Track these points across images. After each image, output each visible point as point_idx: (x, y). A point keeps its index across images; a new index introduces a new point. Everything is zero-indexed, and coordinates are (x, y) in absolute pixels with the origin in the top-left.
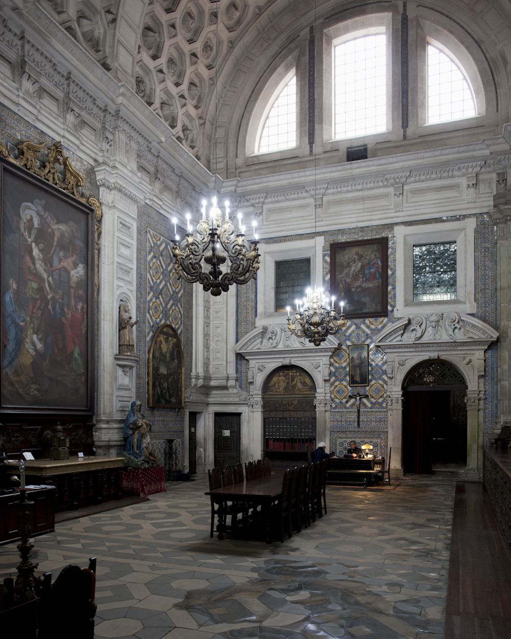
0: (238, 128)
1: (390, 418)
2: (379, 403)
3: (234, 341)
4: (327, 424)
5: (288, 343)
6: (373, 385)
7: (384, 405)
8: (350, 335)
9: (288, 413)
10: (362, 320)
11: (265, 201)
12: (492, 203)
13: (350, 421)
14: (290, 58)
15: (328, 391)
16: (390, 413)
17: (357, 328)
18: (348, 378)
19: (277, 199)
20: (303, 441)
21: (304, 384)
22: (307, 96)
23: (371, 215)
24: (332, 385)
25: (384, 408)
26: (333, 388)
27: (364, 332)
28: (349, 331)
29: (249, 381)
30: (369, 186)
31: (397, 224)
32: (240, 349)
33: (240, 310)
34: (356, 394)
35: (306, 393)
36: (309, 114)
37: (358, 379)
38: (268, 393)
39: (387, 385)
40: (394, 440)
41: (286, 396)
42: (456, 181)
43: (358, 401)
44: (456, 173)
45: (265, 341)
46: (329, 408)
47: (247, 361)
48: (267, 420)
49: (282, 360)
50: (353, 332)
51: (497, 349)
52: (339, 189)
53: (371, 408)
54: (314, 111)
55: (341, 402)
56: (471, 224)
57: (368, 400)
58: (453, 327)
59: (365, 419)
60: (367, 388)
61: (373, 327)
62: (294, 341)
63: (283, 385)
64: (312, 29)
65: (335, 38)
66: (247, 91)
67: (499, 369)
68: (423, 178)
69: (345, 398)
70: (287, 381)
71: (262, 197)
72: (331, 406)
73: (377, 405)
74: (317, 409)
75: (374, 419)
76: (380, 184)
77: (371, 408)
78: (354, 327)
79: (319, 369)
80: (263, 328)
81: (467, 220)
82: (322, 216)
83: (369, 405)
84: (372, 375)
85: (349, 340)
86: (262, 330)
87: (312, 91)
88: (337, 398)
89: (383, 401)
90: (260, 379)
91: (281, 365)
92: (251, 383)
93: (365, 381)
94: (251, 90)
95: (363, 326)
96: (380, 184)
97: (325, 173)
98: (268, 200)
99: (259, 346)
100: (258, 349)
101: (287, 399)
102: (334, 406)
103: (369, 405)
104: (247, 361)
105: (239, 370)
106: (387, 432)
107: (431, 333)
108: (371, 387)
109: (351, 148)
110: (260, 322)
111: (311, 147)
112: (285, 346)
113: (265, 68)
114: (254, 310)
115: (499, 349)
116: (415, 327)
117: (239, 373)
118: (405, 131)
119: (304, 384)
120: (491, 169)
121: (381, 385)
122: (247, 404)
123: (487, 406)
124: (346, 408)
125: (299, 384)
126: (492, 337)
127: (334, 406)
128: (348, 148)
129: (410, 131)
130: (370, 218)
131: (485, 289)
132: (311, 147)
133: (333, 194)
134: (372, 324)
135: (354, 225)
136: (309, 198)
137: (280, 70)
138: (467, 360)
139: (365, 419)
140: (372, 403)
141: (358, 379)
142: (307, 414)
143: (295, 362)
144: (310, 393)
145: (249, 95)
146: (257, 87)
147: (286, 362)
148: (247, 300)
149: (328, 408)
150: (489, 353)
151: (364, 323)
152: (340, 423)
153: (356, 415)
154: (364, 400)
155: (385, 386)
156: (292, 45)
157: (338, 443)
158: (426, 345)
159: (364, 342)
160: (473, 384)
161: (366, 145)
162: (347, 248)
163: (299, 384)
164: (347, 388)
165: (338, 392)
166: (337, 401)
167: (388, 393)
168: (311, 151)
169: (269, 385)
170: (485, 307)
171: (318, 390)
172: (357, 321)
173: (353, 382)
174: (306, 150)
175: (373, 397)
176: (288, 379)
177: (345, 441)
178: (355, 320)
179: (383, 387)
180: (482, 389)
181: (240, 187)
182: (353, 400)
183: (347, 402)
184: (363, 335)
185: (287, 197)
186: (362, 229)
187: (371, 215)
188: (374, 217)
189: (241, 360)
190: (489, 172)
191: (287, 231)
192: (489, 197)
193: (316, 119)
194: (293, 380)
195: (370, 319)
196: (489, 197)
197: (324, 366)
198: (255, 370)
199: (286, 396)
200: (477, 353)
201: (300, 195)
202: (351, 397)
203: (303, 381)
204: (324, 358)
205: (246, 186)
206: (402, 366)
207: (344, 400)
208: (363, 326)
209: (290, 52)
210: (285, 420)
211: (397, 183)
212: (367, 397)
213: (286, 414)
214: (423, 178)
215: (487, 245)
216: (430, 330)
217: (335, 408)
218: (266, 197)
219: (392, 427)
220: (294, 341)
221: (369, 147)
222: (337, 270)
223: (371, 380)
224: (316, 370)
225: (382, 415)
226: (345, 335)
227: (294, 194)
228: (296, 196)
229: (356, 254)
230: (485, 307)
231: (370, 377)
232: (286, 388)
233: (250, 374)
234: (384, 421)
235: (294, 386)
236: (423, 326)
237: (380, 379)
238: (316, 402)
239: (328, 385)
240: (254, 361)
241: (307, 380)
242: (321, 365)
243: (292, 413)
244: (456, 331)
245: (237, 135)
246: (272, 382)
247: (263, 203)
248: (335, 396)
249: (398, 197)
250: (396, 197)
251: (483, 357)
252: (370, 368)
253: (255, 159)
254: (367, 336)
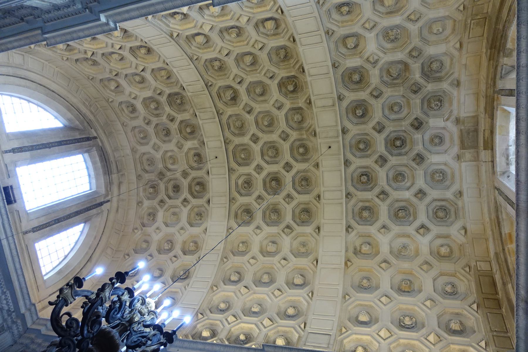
0: (22, 77)
14: (77, 123)
36: (38, 145)
54: (41, 149)
64: (95, 138)
65: (89, 155)
66: (54, 87)
87: (56, 144)
94: (54, 90)
111: (10, 151)
113: (71, 103)
128: (11, 187)
129: (31, 235)
132: (10, 151)
137: (69, 115)
145: (52, 89)
146: (57, 96)
156: (86, 124)
161: (15, 201)
209: (82, 123)
221: (14, 205)
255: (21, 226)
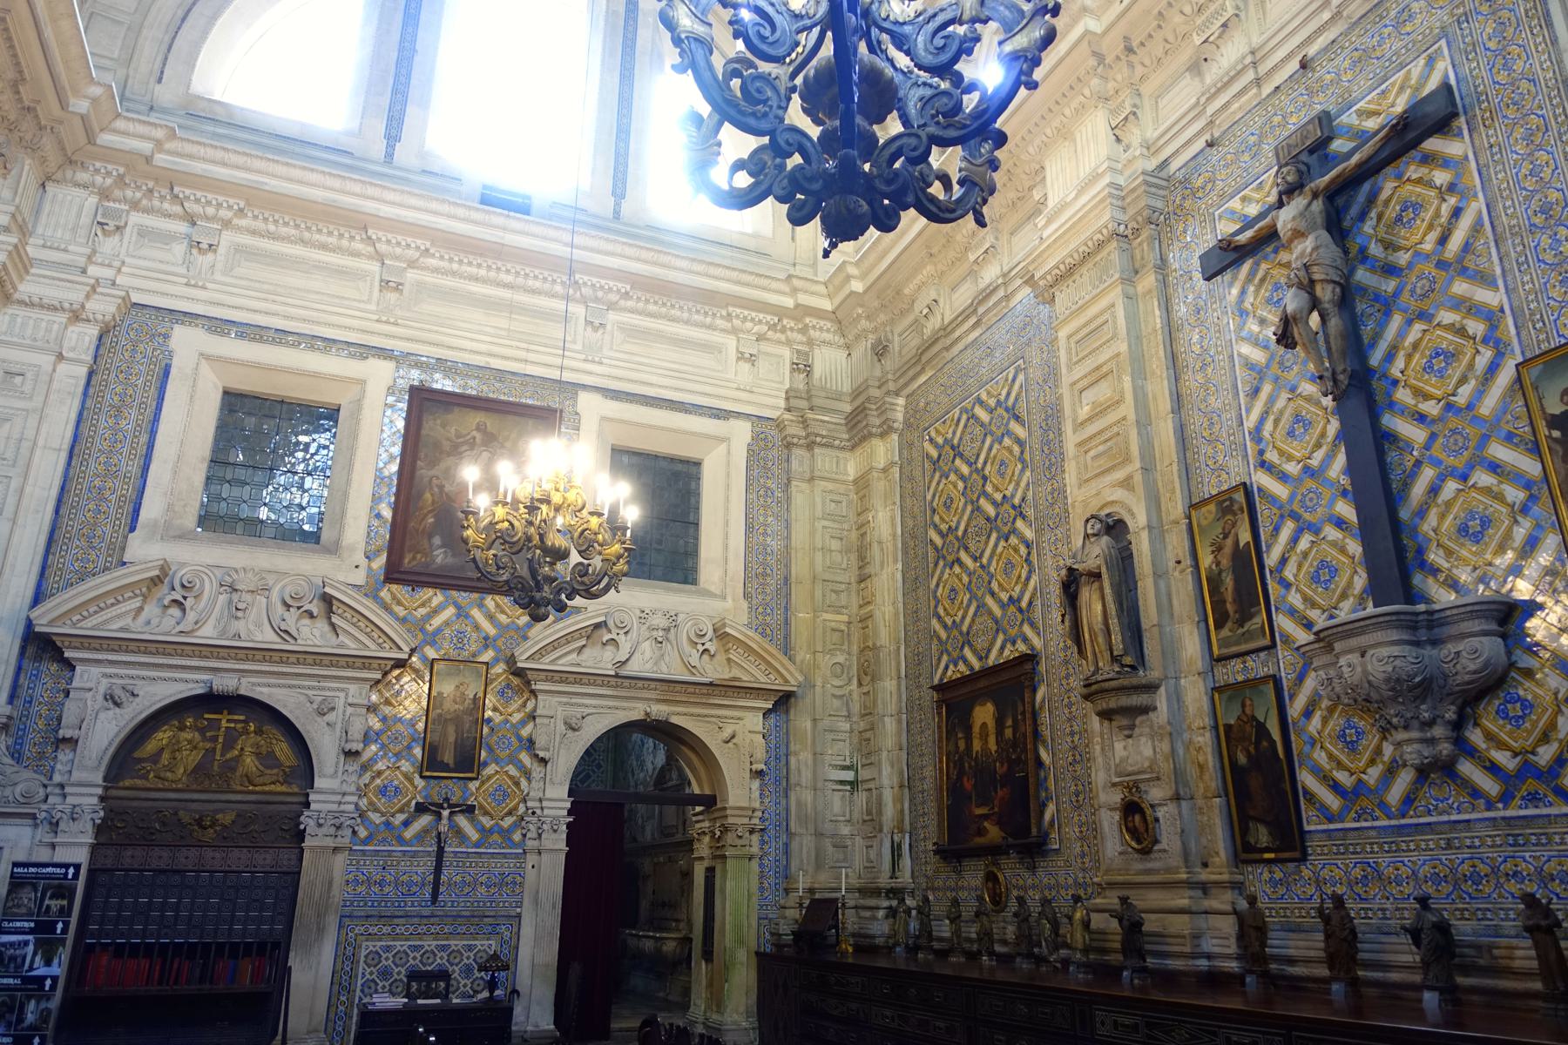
0: (180, 13)
1: (530, 874)
2: (506, 834)
3: (30, 593)
4: (336, 891)
5: (239, 626)
6: (489, 778)
7: (517, 837)
8: (439, 630)
9: (193, 853)
10: (476, 595)
11: (235, 221)
12: (782, 404)
13: (411, 884)
15: (353, 789)
16: (531, 859)
17: (458, 616)
18: (418, 751)
19: (272, 228)
20: (236, 950)
21: (268, 759)
22: (396, 37)
23: (528, 350)
24: (365, 768)
25: (516, 845)
26: (367, 778)
27: (477, 627)
28: (437, 621)
29: (64, 732)
30: (530, 283)
31: (585, 387)
32: (51, 623)
33: (71, 498)
34: (436, 799)
35: (272, 788)
37: (448, 757)
38: (127, 783)
39: (529, 780)
40: (537, 940)
41: (195, 796)
42: (716, 338)
43: (445, 821)
44: (719, 322)
45: (151, 610)
46: (347, 840)
47: (70, 666)
48: (103, 878)
49: (205, 677)
50: (447, 623)
51: (787, 712)
52: (455, 266)
53: (477, 845)
55: (388, 824)
56: (741, 433)
57: (473, 821)
58: (701, 648)
59: (458, 878)
60: (473, 786)
61: (503, 618)
62: (259, 625)
63: (192, 758)
67: (793, 760)
68: (652, 308)
69: (401, 811)
70: (208, 745)
71: (230, 207)
72: (354, 832)
73: (495, 837)
74: (308, 843)
75: (483, 879)
76: (558, 288)
77: (477, 845)
78: (450, 612)
79: (331, 717)
80: (162, 568)
81: (733, 422)
82: (399, 312)
83: (474, 835)
84: (490, 750)
85: (433, 643)
86: (157, 572)
87: (410, 30)
88: (376, 810)
89: (515, 826)
90: (103, 732)
91: (199, 690)
92: (72, 742)
93: (467, 763)
95: (476, 613)
96: (558, 288)
97: (436, 213)
98: (243, 222)
99: (127, 621)
100: (122, 629)
101: (194, 806)
102: (363, 833)
103: (474, 835)
104: (70, 666)
105: (23, 693)
106: (519, 916)
107: (648, 654)
108: (483, 783)
109: (491, 188)
110: (144, 550)
112: (222, 635)
114: (128, 508)
115: (792, 712)
116: (614, 636)
117: (19, 702)
118: (617, 205)
119: (268, 759)
120: (783, 338)
121: (511, 777)
122: (34, 817)
123: (766, 847)
124: (401, 840)
125: (250, 762)
126: (786, 681)
127: (363, 833)
128: (485, 187)
130: (523, 354)
131: (765, 575)
133: (436, 270)
134: (503, 612)
135: (480, 360)
136: (370, 257)
138: (726, 734)
139: (458, 878)
140: (482, 830)
141: (448, 757)
142: (264, 859)
143: (250, 687)
144: (283, 788)
147: (225, 683)
148: (110, 473)
149: (345, 838)
150: (772, 720)
151: (481, 606)
152: (376, 889)
153: (430, 863)
154: (462, 821)
155: (524, 783)
157: (364, 953)
158: (640, 684)
159: (474, 655)
160: (740, 793)
162: (456, 410)
163: (250, 762)
164: (410, 780)
165: (383, 791)
166: (376, 818)
167: (530, 804)
168: (389, 155)
169: (137, 755)
170: (765, 614)
171: (318, 783)
172: (463, 597)
173: (432, 763)
174: (378, 148)
175: (486, 813)
176: (214, 739)
177: (388, 949)
178: (454, 593)
179: (517, 784)
180: (757, 805)
181: (169, 153)
182: (426, 820)
183: (406, 824)
184: (474, 635)
185: (307, 235)
186: (500, 374)
187: (528, 350)
188: (532, 357)
189: (38, 658)
190: (779, 342)
191: (286, 317)
192: (778, 390)
193: (414, 93)
194: (229, 744)
195: (497, 598)
196: (778, 390)
197: (350, 710)
198: (94, 701)
199: (195, 796)
200: (748, 715)
201: (345, 243)
202: (421, 809)
203: (264, 750)
204: (353, 688)
205: (190, 157)
206: (574, 730)
207: (401, 817)
208: (476, 613)
210: (177, 878)
211: (597, 300)
212: (469, 810)
213: (187, 858)
214: (652, 308)
215: (769, 482)
216: (647, 646)
217: (365, 842)
218: (241, 210)
219: (536, 901)
220: (259, 625)
222: (422, 455)
223: (486, 764)
224: (319, 719)
225: (509, 866)
226: (422, 630)
227: (330, 233)
228: (332, 240)
229: (478, 429)
230: (765, 614)
231: (483, 754)
232: (200, 771)
233: (71, 711)
234: (512, 883)
235: (231, 766)
236: (633, 635)
237: (511, 762)
238: (307, 821)
239: (354, 767)
240: (95, 671)
241: (283, 750)
242: (340, 703)
243: (209, 853)
244: (706, 657)
245: (173, 28)
246: (150, 747)
247: (227, 224)
248: (371, 803)
249: (596, 329)
250: (589, 329)
251: (760, 728)
252: (486, 730)
253: (219, 109)
254: (487, 642)
255: (595, 216)
